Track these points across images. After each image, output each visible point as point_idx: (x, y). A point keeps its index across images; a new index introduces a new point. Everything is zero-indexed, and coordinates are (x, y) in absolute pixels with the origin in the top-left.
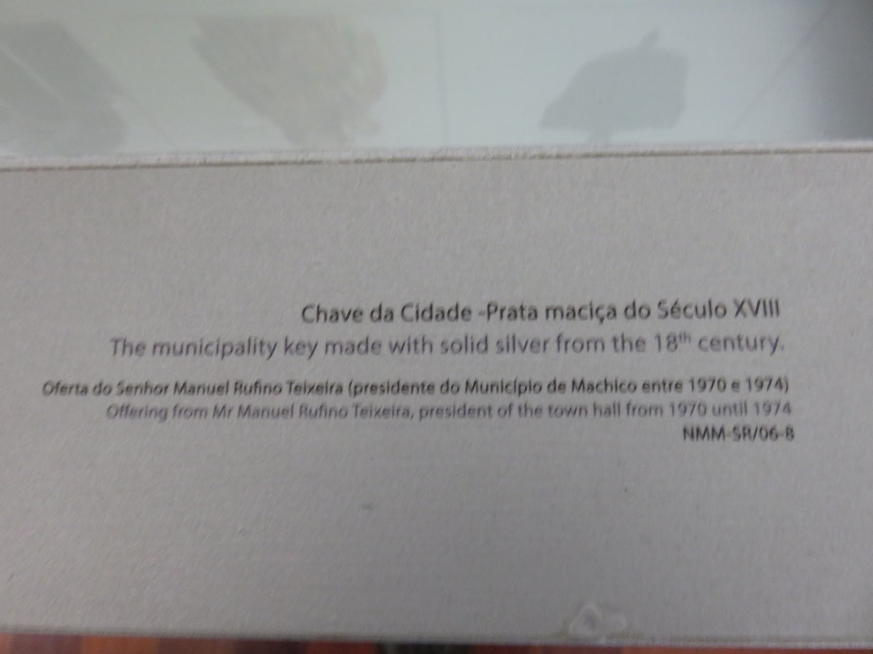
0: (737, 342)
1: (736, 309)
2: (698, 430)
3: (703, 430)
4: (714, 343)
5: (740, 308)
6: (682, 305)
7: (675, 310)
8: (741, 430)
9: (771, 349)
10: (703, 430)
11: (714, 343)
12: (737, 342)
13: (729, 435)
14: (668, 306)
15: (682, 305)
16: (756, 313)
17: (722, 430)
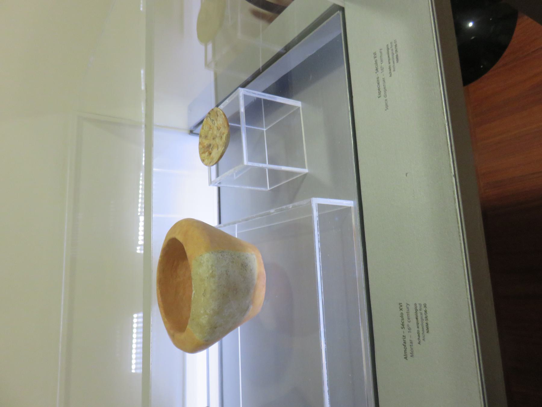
0: (408, 313)
1: (401, 311)
2: (427, 329)
3: (427, 328)
4: (409, 319)
5: (401, 309)
6: (402, 323)
7: (403, 325)
8: (426, 319)
9: (408, 305)
10: (427, 328)
11: (409, 319)
12: (408, 313)
13: (427, 322)
14: (402, 327)
15: (402, 323)
16: (402, 306)
17: (426, 323)
